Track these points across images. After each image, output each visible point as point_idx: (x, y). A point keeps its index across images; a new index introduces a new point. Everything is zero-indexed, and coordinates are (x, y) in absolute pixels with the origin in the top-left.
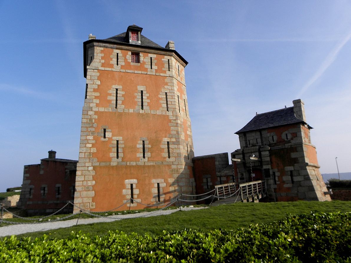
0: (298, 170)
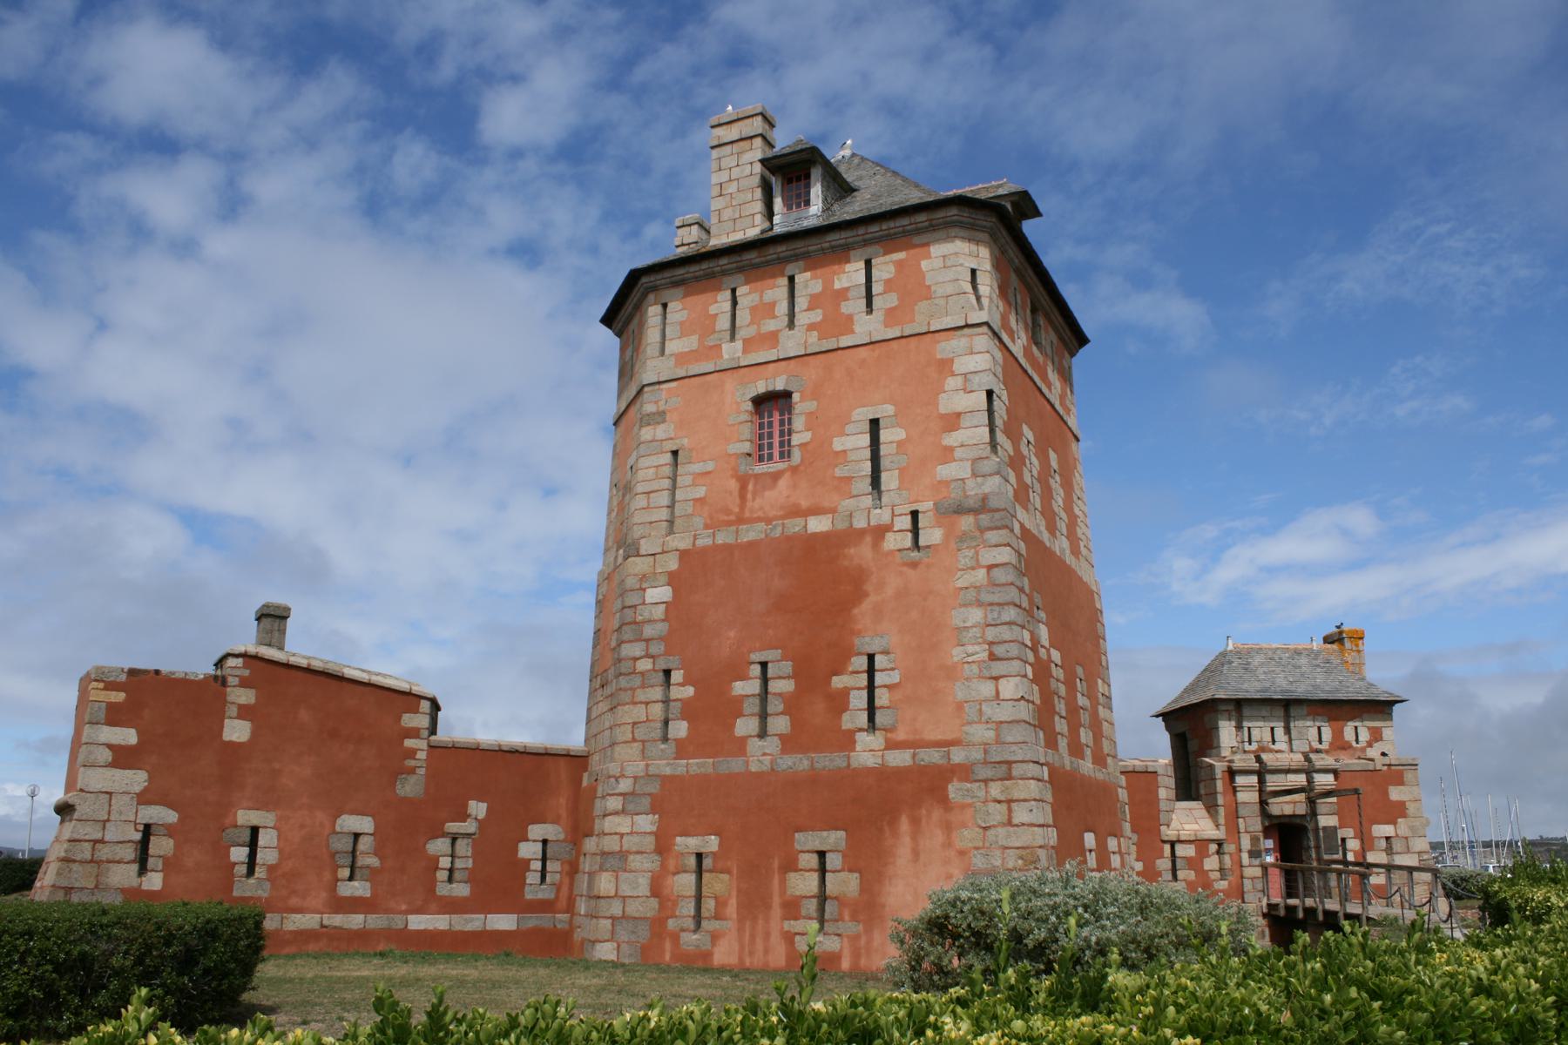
0: (1406, 838)
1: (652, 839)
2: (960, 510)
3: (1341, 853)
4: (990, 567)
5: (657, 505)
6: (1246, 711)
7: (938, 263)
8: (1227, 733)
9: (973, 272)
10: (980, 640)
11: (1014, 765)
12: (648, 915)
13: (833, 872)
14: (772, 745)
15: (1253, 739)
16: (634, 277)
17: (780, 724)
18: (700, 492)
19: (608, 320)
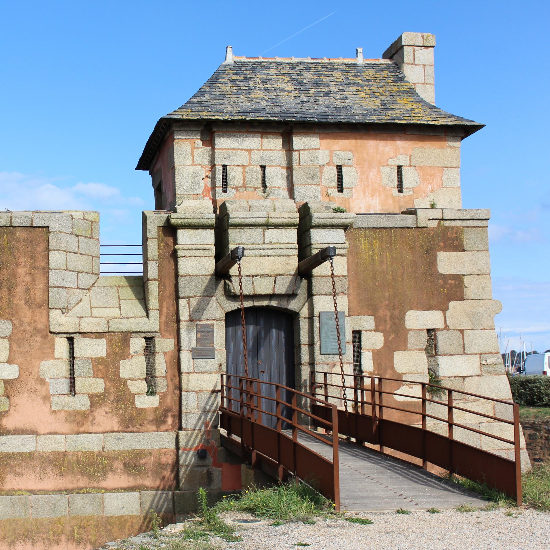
0: (462, 331)
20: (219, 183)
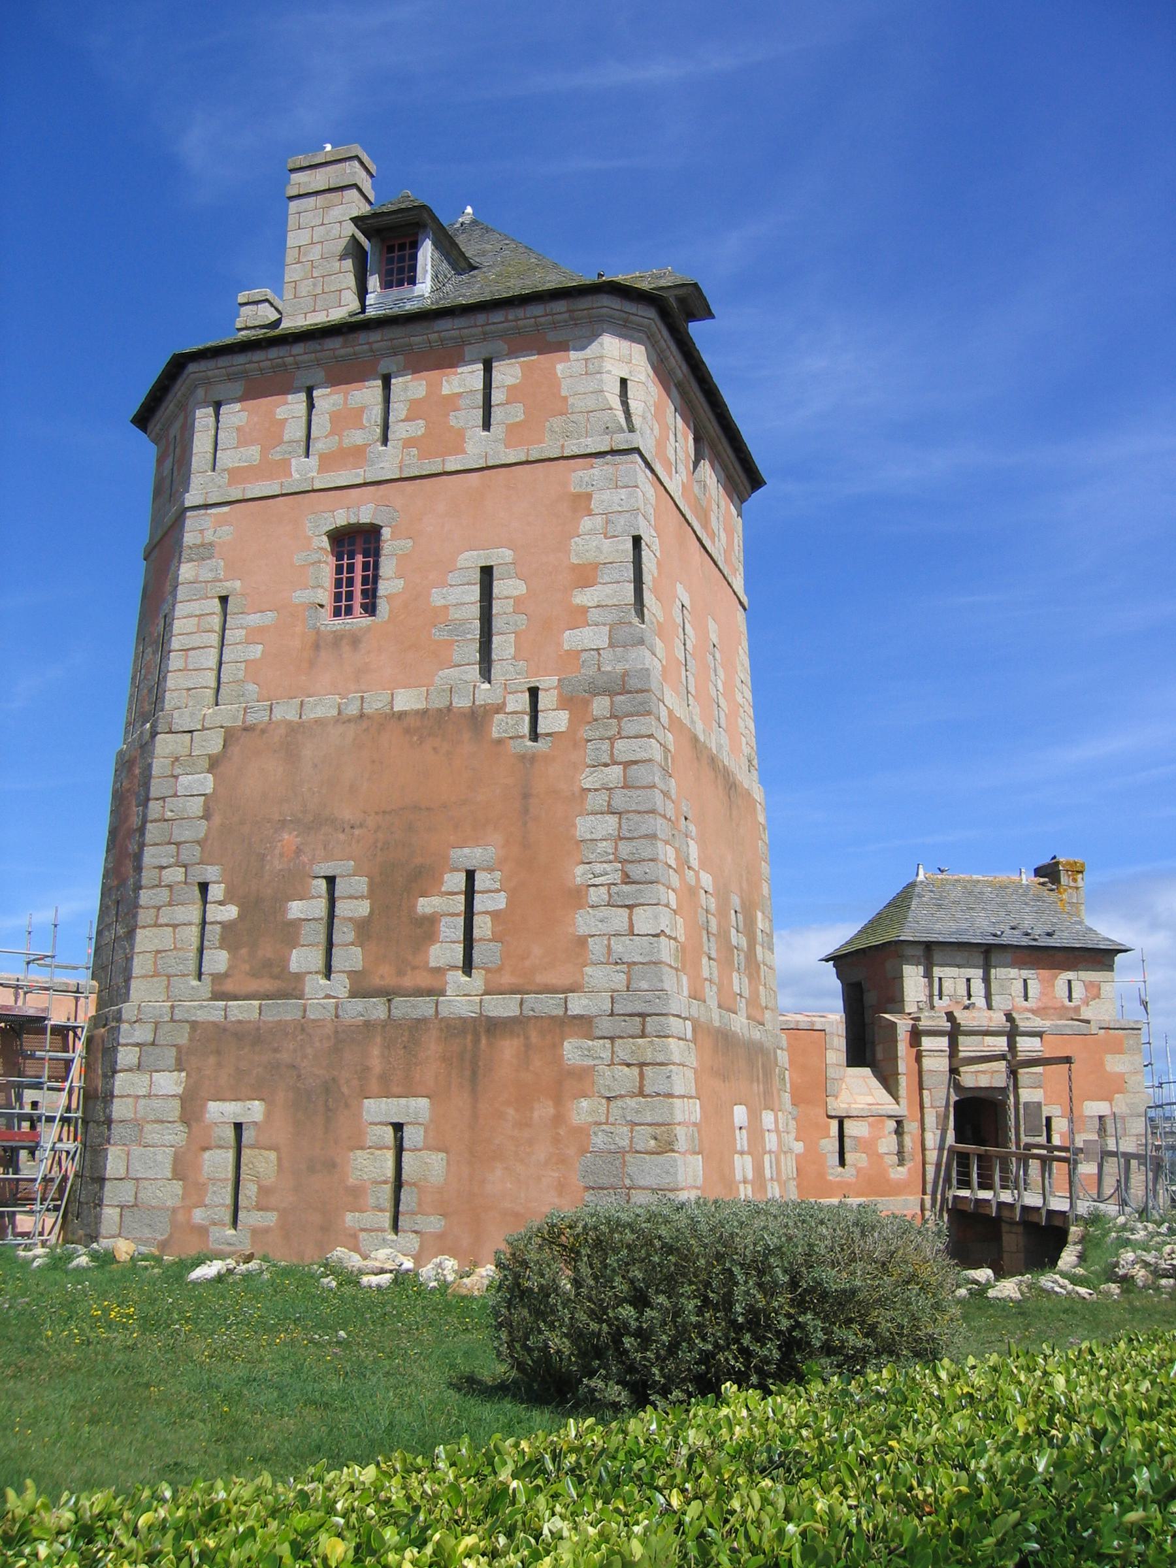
1: (177, 1103)
2: (596, 690)
3: (1045, 1134)
4: (627, 764)
5: (197, 666)
6: (937, 956)
7: (578, 367)
8: (913, 981)
9: (624, 382)
10: (611, 857)
11: (648, 1019)
12: (169, 1203)
13: (412, 1151)
14: (340, 985)
15: (945, 991)
16: (178, 364)
17: (349, 957)
18: (256, 651)
19: (142, 420)
20: (936, 992)
